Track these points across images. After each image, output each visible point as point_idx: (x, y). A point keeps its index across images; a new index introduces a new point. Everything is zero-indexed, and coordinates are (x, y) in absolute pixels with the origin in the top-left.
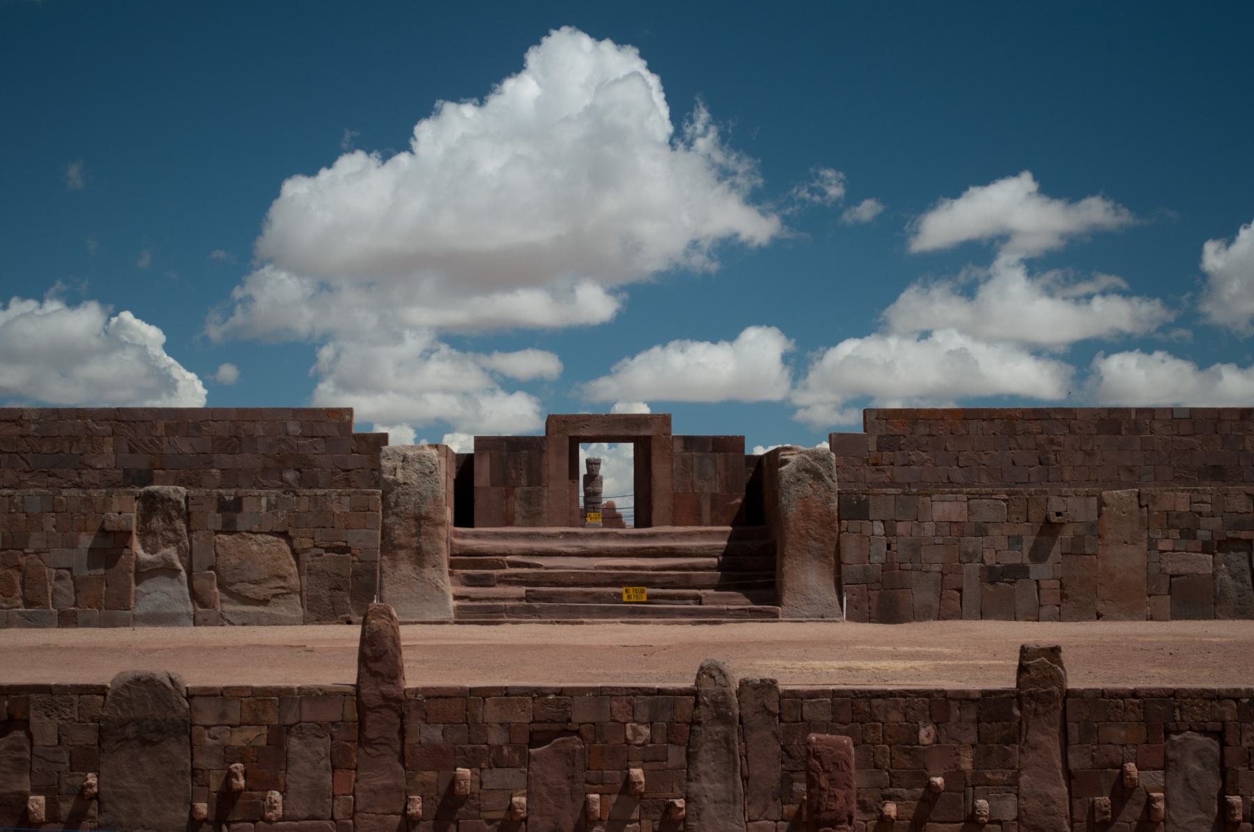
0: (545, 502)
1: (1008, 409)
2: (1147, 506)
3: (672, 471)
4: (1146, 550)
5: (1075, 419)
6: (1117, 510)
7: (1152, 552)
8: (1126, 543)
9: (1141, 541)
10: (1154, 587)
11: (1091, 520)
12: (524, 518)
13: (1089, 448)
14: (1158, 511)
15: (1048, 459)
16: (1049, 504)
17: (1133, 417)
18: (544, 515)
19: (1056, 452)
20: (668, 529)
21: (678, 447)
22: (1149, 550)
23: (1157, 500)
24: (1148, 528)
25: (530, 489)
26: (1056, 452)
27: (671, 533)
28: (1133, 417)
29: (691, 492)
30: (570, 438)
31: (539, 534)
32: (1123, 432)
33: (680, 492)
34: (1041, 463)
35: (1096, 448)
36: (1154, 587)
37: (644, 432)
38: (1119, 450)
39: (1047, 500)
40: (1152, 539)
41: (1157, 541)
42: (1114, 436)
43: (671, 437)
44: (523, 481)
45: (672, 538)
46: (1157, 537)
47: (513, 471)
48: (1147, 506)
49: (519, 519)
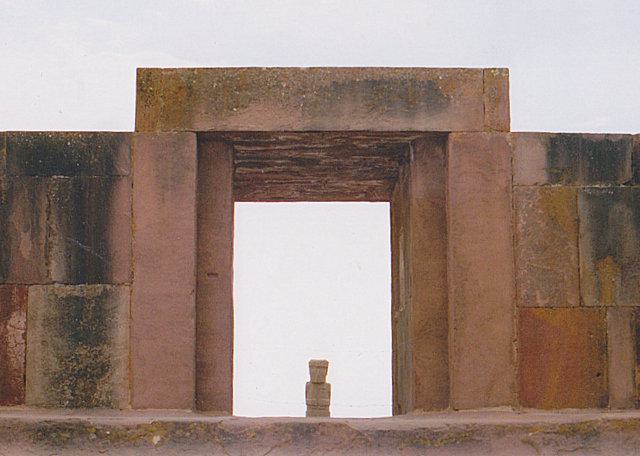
0: (121, 332)
3: (515, 239)
12: (57, 380)
18: (119, 373)
20: (506, 416)
21: (531, 168)
25: (76, 290)
27: (527, 428)
29: (573, 301)
30: (203, 138)
31: (82, 429)
33: (541, 302)
37: (425, 123)
43: (508, 137)
44: (56, 269)
45: (529, 443)
47: (25, 237)
49: (36, 389)
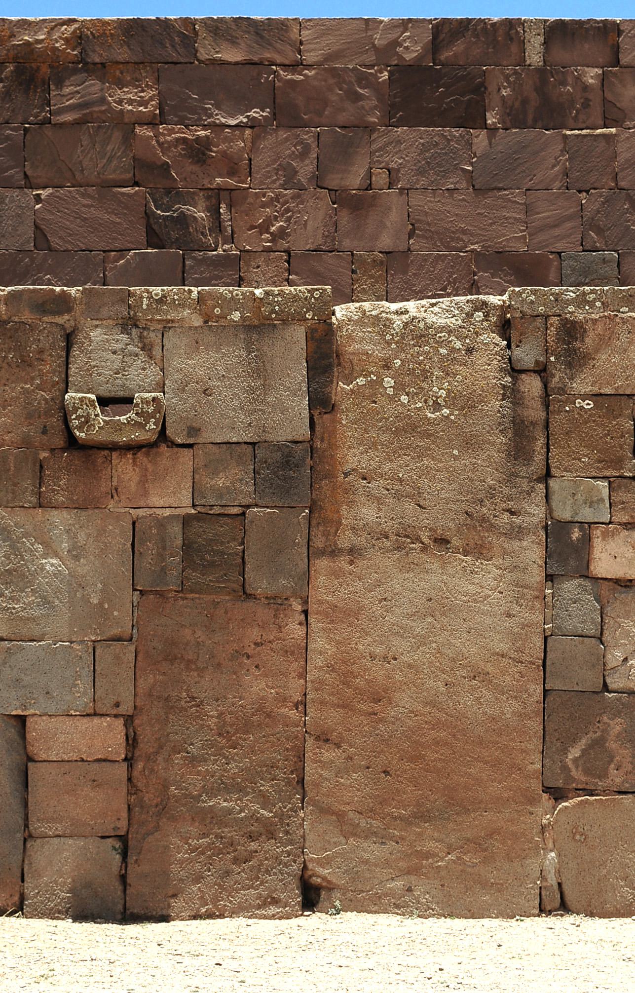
1: (24, 24)
2: (542, 370)
4: (536, 575)
5: (295, 66)
6: (400, 387)
7: (570, 587)
8: (442, 542)
9: (518, 532)
10: (575, 752)
11: (283, 435)
13: (354, 180)
14: (596, 396)
15: (183, 220)
16: (78, 358)
17: (534, 56)
19: (216, 196)
22: (550, 578)
23: (590, 341)
24: (548, 475)
26: (216, 196)
28: (534, 56)
32: (491, 119)
34: (154, 239)
35: (380, 178)
36: (575, 752)
38: (480, 191)
39: (69, 339)
40: (564, 526)
41: (587, 540)
42: (456, 132)
46: (587, 514)
48: (542, 370)
